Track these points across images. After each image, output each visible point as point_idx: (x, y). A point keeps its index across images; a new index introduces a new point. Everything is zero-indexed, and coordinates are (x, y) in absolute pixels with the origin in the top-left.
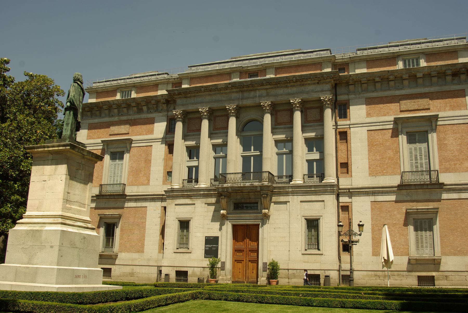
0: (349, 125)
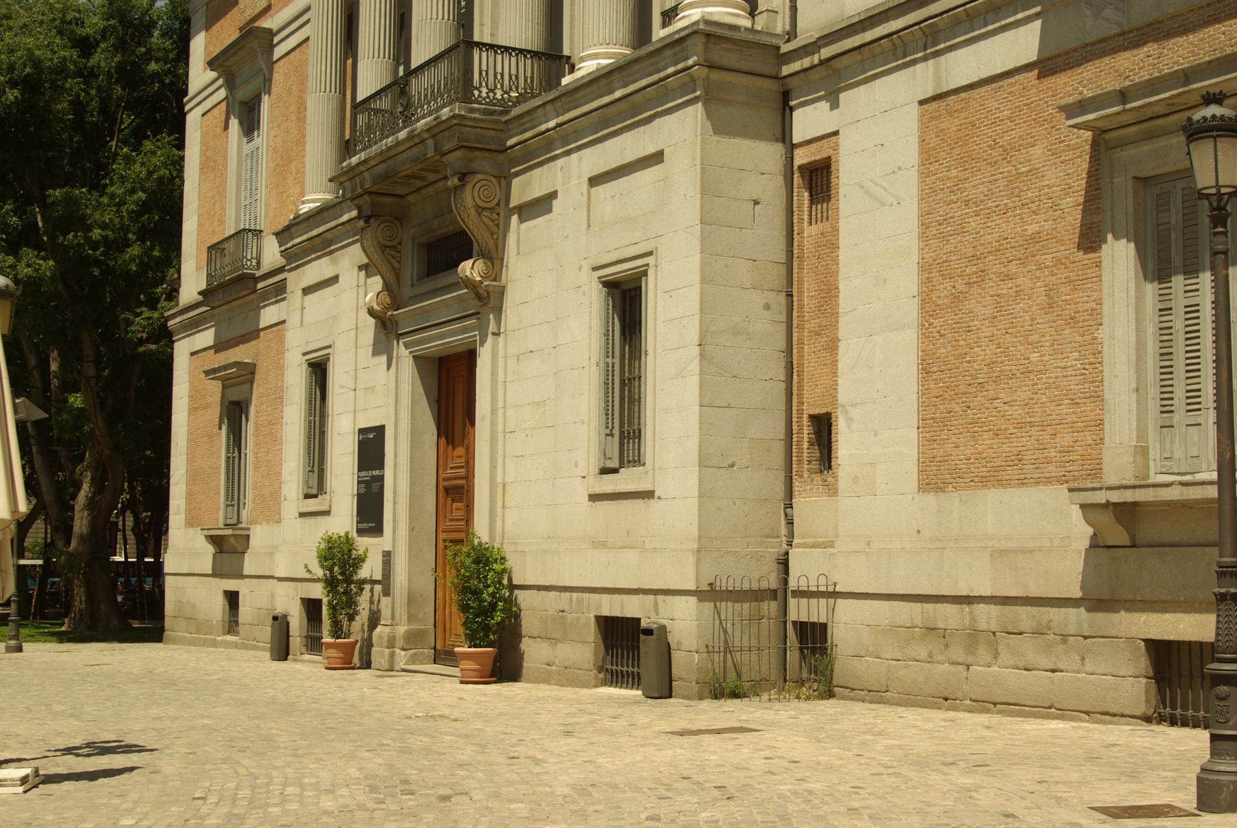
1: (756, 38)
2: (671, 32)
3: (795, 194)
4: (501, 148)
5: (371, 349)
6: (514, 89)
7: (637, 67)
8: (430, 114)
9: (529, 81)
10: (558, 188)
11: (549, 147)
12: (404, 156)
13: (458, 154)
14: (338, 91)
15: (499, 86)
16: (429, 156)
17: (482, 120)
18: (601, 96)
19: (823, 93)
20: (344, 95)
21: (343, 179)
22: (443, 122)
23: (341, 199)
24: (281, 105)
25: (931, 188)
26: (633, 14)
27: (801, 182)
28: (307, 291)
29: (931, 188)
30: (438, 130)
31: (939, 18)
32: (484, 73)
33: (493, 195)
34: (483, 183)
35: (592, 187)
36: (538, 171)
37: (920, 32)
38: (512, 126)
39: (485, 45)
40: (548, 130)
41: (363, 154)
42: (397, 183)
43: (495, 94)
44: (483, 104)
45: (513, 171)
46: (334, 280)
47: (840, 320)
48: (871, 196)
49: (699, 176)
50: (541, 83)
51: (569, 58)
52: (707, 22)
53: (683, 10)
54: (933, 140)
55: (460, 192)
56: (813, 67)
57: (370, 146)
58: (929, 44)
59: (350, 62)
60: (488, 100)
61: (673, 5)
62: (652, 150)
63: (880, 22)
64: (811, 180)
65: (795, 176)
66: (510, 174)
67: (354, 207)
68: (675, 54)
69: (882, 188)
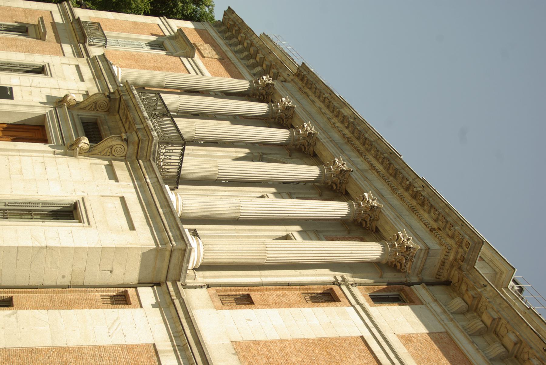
0: (358, 303)
1: (183, 271)
2: (187, 234)
3: (115, 289)
4: (138, 158)
5: (50, 95)
6: (164, 164)
7: (172, 219)
8: (154, 127)
9: (167, 170)
10: (120, 183)
11: (139, 179)
12: (136, 114)
13: (136, 139)
14: (166, 85)
15: (166, 157)
16: (136, 125)
17: (151, 150)
18: (160, 203)
19: (159, 301)
20: (164, 88)
21: (127, 87)
22: (150, 132)
23: (118, 85)
24: (161, 59)
25: (116, 350)
26: (195, 217)
27: (120, 291)
28: (77, 67)
29: (116, 350)
30: (147, 130)
31: (191, 352)
32: (171, 151)
33: (117, 153)
34: (123, 149)
35: (120, 198)
36: (128, 174)
37: (185, 344)
38: (148, 162)
39: (184, 152)
40: (145, 179)
41: (138, 96)
42: (124, 111)
43: (162, 156)
44: (158, 150)
45: (128, 162)
46: (82, 80)
47: (57, 310)
48: (113, 323)
49: (124, 246)
50: (166, 175)
51: (177, 188)
52: (191, 250)
53: (196, 239)
54: (137, 351)
55: (119, 139)
56: (171, 296)
57: (141, 99)
58: (180, 347)
59: (179, 91)
60: (160, 152)
61: (199, 234)
62: (136, 225)
63: (189, 326)
64: (121, 296)
65: (123, 289)
66: (127, 161)
67: (115, 90)
68: (177, 236)
69: (117, 328)
